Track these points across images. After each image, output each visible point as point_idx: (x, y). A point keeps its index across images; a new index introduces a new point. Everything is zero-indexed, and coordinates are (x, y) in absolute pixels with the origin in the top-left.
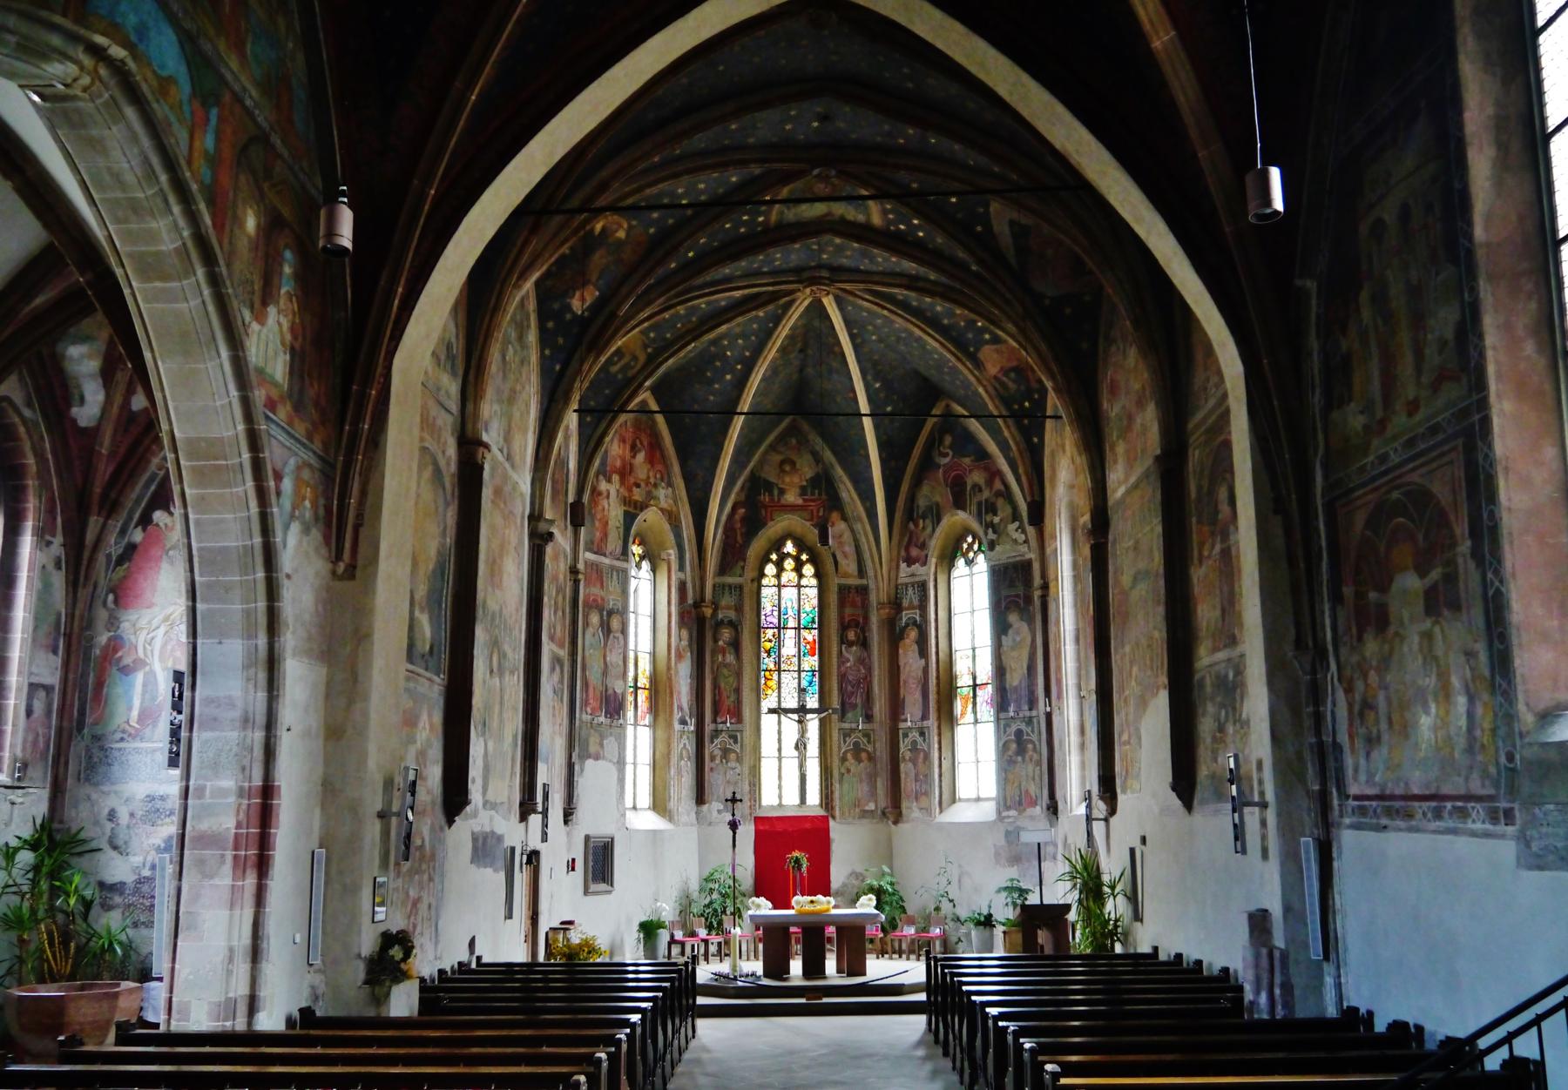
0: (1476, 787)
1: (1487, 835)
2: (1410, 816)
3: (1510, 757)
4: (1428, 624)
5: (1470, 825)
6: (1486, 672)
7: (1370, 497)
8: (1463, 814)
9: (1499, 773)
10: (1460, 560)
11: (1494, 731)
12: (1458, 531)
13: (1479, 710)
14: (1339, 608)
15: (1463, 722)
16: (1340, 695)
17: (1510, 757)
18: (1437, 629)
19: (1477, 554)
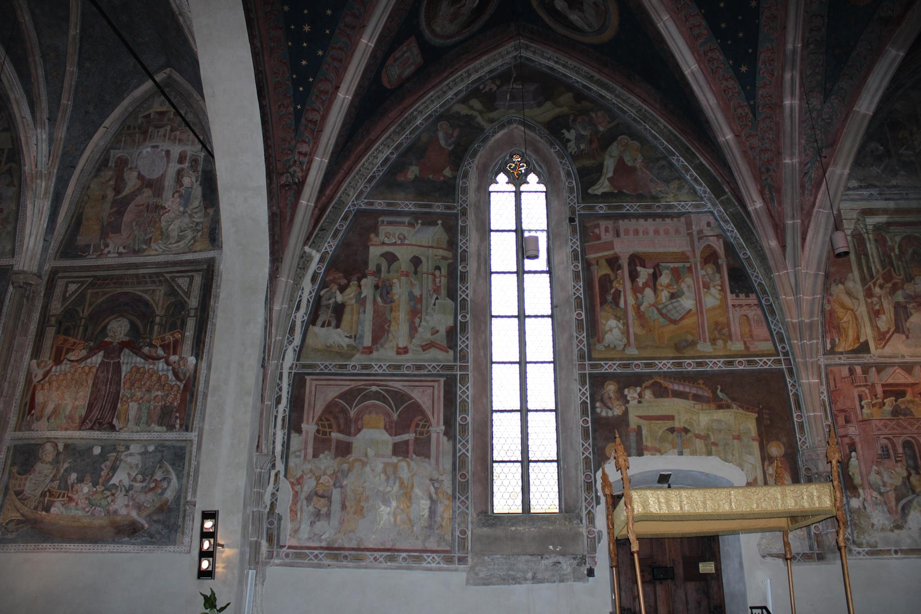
0: (432, 544)
1: (440, 570)
2: (358, 559)
4: (395, 460)
5: (424, 564)
6: (450, 491)
7: (348, 383)
8: (419, 559)
9: (453, 540)
10: (434, 436)
11: (453, 519)
12: (433, 421)
13: (440, 508)
14: (294, 436)
15: (426, 513)
16: (285, 485)
17: (463, 532)
18: (404, 464)
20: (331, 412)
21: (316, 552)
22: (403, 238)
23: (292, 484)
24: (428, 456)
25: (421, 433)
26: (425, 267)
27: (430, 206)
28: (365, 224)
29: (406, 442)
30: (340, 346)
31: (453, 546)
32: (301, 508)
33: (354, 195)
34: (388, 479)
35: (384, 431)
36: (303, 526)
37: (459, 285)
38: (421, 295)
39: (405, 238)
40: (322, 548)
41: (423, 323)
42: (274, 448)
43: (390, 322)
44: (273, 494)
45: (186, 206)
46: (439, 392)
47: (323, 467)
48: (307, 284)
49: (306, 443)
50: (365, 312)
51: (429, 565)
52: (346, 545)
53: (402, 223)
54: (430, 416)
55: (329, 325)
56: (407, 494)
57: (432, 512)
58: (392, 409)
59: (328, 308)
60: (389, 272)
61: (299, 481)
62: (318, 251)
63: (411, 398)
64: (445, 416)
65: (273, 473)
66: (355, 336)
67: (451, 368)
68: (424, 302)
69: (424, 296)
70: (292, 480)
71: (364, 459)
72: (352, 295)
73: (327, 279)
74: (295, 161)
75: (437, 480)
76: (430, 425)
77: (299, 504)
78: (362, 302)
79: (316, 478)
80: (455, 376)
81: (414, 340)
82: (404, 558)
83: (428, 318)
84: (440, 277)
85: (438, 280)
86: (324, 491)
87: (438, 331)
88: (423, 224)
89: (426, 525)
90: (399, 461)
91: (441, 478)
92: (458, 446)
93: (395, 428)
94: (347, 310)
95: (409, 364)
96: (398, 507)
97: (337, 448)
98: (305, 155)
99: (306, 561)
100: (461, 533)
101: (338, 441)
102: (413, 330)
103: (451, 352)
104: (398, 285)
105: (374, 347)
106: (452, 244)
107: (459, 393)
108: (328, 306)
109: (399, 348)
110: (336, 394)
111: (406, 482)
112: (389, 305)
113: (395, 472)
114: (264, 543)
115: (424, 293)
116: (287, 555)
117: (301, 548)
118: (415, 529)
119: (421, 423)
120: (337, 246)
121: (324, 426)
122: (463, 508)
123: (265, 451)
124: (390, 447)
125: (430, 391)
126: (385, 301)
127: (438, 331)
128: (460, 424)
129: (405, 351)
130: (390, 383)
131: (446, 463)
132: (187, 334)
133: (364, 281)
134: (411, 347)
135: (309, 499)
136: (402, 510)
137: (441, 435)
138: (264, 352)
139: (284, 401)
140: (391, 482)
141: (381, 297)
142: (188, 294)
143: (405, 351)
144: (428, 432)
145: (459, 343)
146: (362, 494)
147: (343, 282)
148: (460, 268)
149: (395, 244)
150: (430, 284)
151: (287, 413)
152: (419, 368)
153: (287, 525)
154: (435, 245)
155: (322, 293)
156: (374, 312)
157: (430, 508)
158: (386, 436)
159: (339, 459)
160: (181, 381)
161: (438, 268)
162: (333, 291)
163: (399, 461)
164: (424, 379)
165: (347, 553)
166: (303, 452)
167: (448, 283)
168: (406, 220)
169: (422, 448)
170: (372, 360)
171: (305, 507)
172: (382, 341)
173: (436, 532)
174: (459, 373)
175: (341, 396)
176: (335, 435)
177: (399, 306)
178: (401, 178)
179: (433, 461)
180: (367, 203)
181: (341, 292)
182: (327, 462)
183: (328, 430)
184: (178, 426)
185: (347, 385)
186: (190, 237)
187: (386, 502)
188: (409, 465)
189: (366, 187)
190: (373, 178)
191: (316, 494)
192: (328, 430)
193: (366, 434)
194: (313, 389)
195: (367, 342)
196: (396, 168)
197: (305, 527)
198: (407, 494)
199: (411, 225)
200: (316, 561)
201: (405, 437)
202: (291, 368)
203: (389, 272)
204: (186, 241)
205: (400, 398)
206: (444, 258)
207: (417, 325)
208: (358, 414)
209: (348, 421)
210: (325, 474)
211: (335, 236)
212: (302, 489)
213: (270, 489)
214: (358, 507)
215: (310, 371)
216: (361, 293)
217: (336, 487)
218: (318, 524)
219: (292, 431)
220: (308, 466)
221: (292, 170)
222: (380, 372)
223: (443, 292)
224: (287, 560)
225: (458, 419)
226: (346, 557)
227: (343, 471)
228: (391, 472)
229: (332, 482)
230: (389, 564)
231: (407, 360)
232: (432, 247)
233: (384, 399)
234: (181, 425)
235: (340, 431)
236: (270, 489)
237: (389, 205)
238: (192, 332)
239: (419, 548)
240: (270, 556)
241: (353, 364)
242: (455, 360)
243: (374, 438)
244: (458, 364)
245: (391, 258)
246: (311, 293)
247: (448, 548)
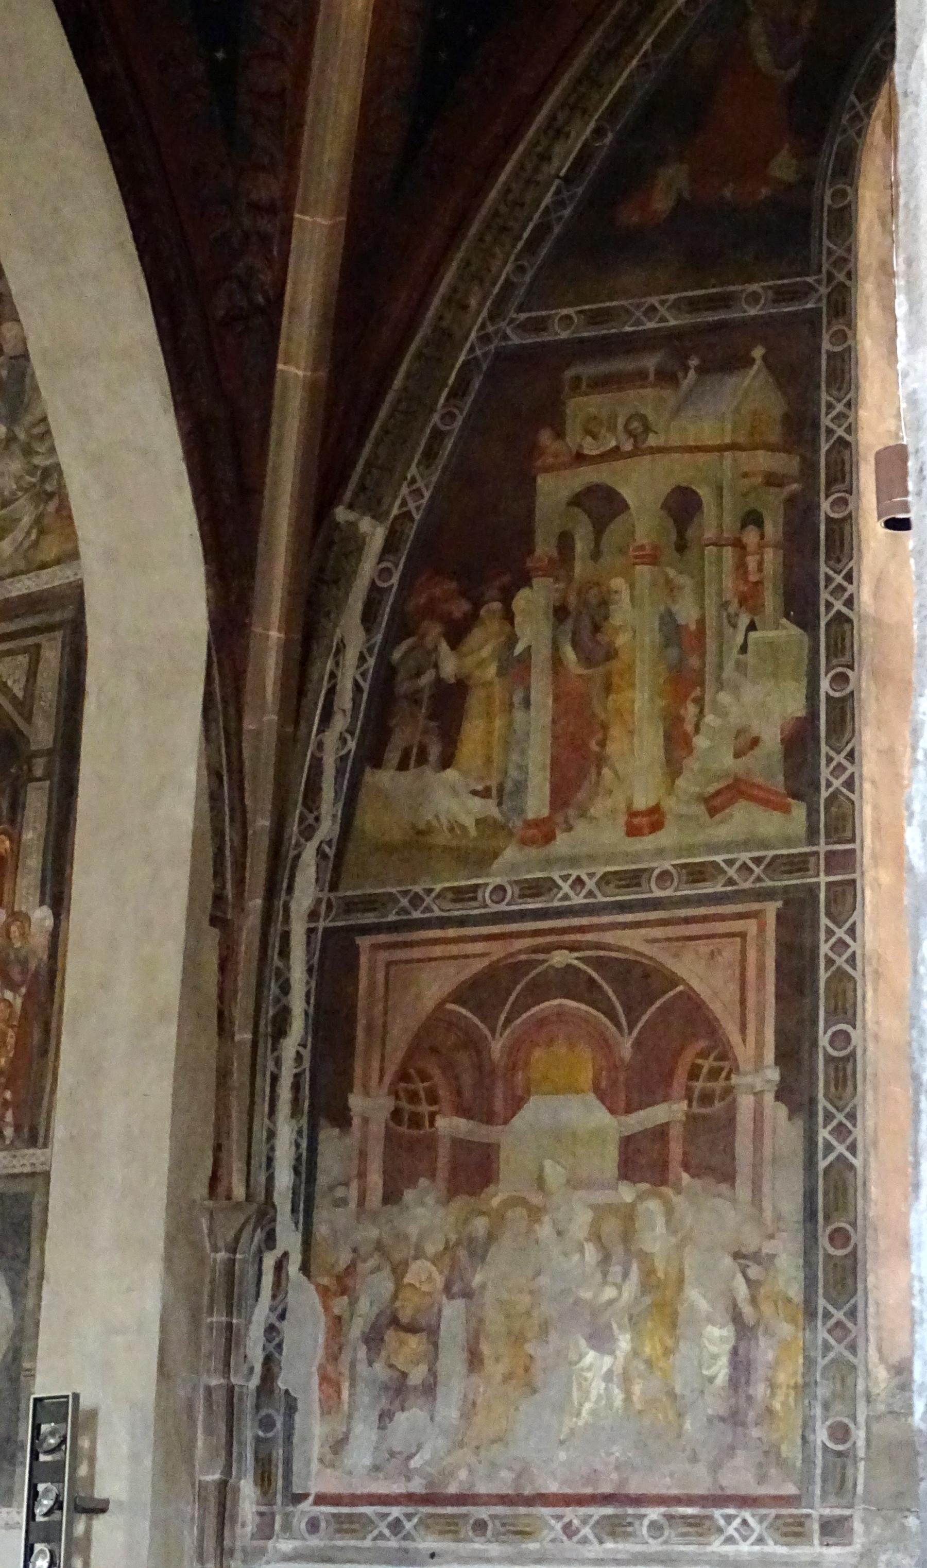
0: (739, 1477)
3: (841, 1433)
4: (627, 1193)
6: (795, 1292)
7: (479, 947)
9: (808, 1460)
10: (745, 1103)
11: (805, 1388)
12: (744, 1052)
13: (764, 1352)
14: (328, 1135)
15: (721, 1371)
16: (304, 1297)
17: (841, 1433)
18: (653, 1205)
19: (795, 1094)
20: (434, 1050)
21: (396, 1512)
22: (640, 428)
23: (324, 1292)
24: (729, 1177)
25: (707, 1098)
26: (714, 519)
27: (725, 301)
28: (523, 399)
29: (661, 1133)
30: (455, 827)
31: (805, 1480)
32: (353, 1365)
33: (478, 307)
34: (606, 1259)
35: (591, 1097)
36: (359, 1428)
37: (824, 569)
38: (701, 622)
39: (647, 429)
40: (410, 1499)
41: (710, 718)
42: (270, 1179)
43: (605, 727)
44: (271, 1330)
45: (12, 419)
46: (761, 951)
47: (413, 1230)
48: (350, 630)
49: (363, 1155)
50: (527, 703)
51: (729, 1549)
52: (482, 1488)
53: (640, 377)
54: (735, 1038)
55: (422, 759)
56: (661, 1307)
57: (741, 1366)
58: (618, 1025)
59: (417, 702)
60: (596, 554)
61: (343, 1284)
62: (378, 517)
63: (673, 980)
64: (779, 1032)
65: (269, 1261)
66: (501, 788)
67: (798, 865)
68: (711, 645)
69: (711, 623)
70: (325, 1281)
71: (536, 1199)
72: (485, 652)
73: (411, 606)
74: (247, 236)
75: (756, 1257)
76: (735, 1069)
77: (345, 1358)
78: (515, 667)
79: (394, 1271)
80: (812, 890)
81: (681, 782)
82: (653, 1525)
83: (724, 697)
84: (761, 547)
85: (752, 562)
86: (418, 1310)
87: (755, 742)
88: (698, 369)
89: (722, 1411)
90: (640, 1197)
91: (768, 1248)
92: (824, 1134)
93: (625, 1088)
94: (475, 702)
95: (667, 865)
96: (636, 1353)
97: (455, 1169)
98: (271, 209)
99: (368, 1543)
100: (832, 1436)
101: (458, 1143)
102: (677, 743)
103: (799, 811)
104: (625, 596)
105: (559, 818)
106: (800, 428)
107: (824, 949)
108: (414, 699)
109: (633, 814)
110: (448, 988)
111: (660, 1266)
112: (601, 670)
113: (627, 1236)
114: (247, 1489)
115: (711, 612)
116: (313, 1525)
117: (355, 1500)
118: (688, 1426)
119: (707, 1064)
120: (438, 489)
121: (413, 1097)
122: (839, 1349)
123: (239, 1192)
124: (612, 1153)
125: (730, 951)
126: (587, 660)
127: (755, 742)
128: (829, 1059)
129: (650, 820)
130: (609, 937)
131: (785, 1195)
132: (29, 836)
133: (522, 600)
134: (670, 804)
135: (374, 1339)
136: (649, 1363)
137: (769, 1098)
138: (218, 873)
139: (297, 1027)
140: (616, 1269)
141: (575, 645)
142: (25, 706)
143: (650, 820)
144: (729, 1091)
145: (825, 772)
146: (528, 1313)
147: (460, 608)
148: (825, 506)
149: (615, 454)
150: (728, 583)
151: (306, 1064)
152: (697, 874)
153: (313, 1429)
154: (741, 440)
155: (397, 655)
156: (556, 699)
157: (735, 1352)
158: (601, 1117)
159: (460, 1202)
160: (14, 988)
161: (753, 519)
162: (429, 642)
163: (640, 1197)
164: (702, 911)
165: (483, 1513)
166: (354, 1184)
167: (787, 566)
168: (651, 362)
169: (709, 1150)
170: (549, 863)
171: (362, 1368)
172: (581, 795)
173: (755, 1433)
174: (823, 879)
175: (466, 993)
176: (449, 1125)
177: (631, 668)
178: (629, 216)
179: (743, 1191)
180: (523, 327)
181: (454, 645)
182: (427, 1215)
183: (424, 1108)
184: (9, 1132)
185: (480, 954)
186: (26, 520)
187: (600, 1339)
188: (669, 1211)
189: (521, 269)
190: (543, 229)
191: (395, 1321)
192: (424, 1108)
193: (536, 1112)
194: (380, 976)
195: (537, 803)
196: (614, 181)
197: (364, 1434)
198: (661, 1307)
199: (667, 378)
200: (393, 1543)
201: (658, 1114)
202: (313, 915)
203: (596, 554)
204: (18, 534)
205: (639, 982)
206: (773, 480)
207: (689, 728)
208: (513, 1049)
209: (484, 1072)
210: (419, 1254)
211: (430, 455)
212: (353, 1303)
213: (262, 1312)
214: (516, 1356)
215: (369, 919)
216: (512, 640)
217: (451, 1297)
218: (401, 1418)
219: (323, 1122)
220: (373, 1233)
221: (239, 268)
222: (578, 900)
223: (771, 600)
224: (315, 1542)
225: (824, 1040)
226: (480, 1526)
227: (471, 1240)
228: (617, 1239)
229: (439, 1281)
230: (610, 1545)
231: (660, 850)
232: (733, 447)
233: (587, 990)
234: (18, 1128)
235: (463, 1111)
236: (262, 1312)
237: (595, 318)
238: (41, 827)
239: (701, 1490)
240: (266, 1530)
241: (498, 881)
242: (812, 834)
243: (564, 1125)
244: (823, 847)
245: (602, 505)
246: (362, 659)
247: (790, 1489)
